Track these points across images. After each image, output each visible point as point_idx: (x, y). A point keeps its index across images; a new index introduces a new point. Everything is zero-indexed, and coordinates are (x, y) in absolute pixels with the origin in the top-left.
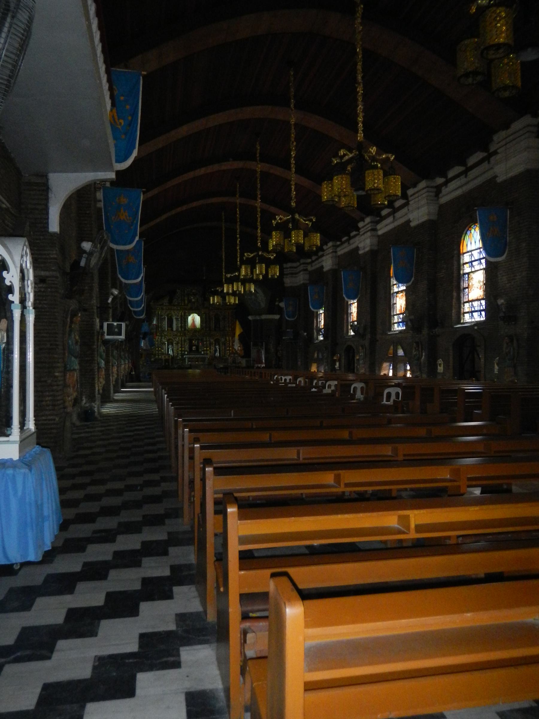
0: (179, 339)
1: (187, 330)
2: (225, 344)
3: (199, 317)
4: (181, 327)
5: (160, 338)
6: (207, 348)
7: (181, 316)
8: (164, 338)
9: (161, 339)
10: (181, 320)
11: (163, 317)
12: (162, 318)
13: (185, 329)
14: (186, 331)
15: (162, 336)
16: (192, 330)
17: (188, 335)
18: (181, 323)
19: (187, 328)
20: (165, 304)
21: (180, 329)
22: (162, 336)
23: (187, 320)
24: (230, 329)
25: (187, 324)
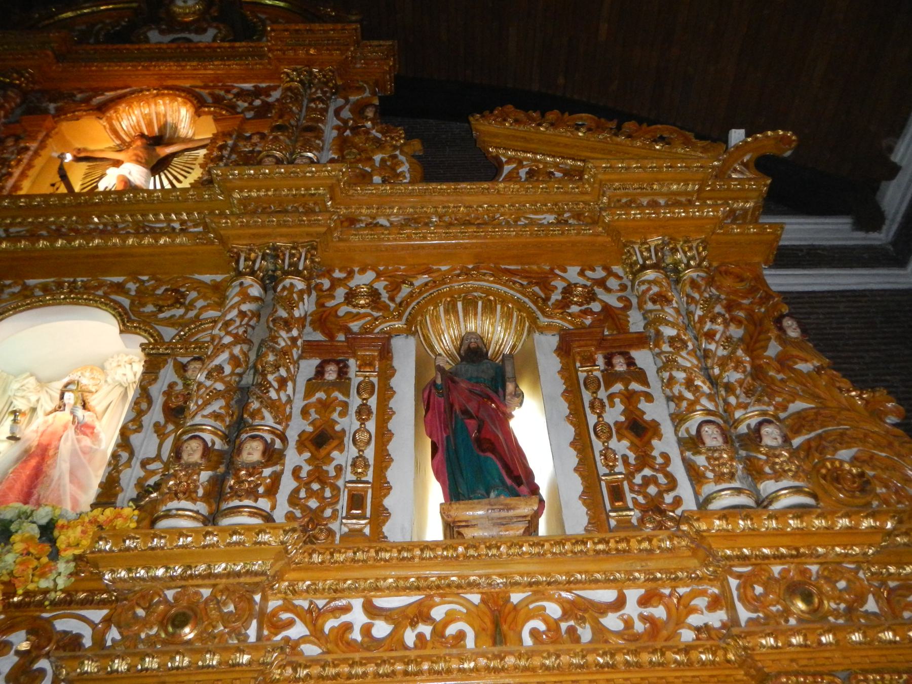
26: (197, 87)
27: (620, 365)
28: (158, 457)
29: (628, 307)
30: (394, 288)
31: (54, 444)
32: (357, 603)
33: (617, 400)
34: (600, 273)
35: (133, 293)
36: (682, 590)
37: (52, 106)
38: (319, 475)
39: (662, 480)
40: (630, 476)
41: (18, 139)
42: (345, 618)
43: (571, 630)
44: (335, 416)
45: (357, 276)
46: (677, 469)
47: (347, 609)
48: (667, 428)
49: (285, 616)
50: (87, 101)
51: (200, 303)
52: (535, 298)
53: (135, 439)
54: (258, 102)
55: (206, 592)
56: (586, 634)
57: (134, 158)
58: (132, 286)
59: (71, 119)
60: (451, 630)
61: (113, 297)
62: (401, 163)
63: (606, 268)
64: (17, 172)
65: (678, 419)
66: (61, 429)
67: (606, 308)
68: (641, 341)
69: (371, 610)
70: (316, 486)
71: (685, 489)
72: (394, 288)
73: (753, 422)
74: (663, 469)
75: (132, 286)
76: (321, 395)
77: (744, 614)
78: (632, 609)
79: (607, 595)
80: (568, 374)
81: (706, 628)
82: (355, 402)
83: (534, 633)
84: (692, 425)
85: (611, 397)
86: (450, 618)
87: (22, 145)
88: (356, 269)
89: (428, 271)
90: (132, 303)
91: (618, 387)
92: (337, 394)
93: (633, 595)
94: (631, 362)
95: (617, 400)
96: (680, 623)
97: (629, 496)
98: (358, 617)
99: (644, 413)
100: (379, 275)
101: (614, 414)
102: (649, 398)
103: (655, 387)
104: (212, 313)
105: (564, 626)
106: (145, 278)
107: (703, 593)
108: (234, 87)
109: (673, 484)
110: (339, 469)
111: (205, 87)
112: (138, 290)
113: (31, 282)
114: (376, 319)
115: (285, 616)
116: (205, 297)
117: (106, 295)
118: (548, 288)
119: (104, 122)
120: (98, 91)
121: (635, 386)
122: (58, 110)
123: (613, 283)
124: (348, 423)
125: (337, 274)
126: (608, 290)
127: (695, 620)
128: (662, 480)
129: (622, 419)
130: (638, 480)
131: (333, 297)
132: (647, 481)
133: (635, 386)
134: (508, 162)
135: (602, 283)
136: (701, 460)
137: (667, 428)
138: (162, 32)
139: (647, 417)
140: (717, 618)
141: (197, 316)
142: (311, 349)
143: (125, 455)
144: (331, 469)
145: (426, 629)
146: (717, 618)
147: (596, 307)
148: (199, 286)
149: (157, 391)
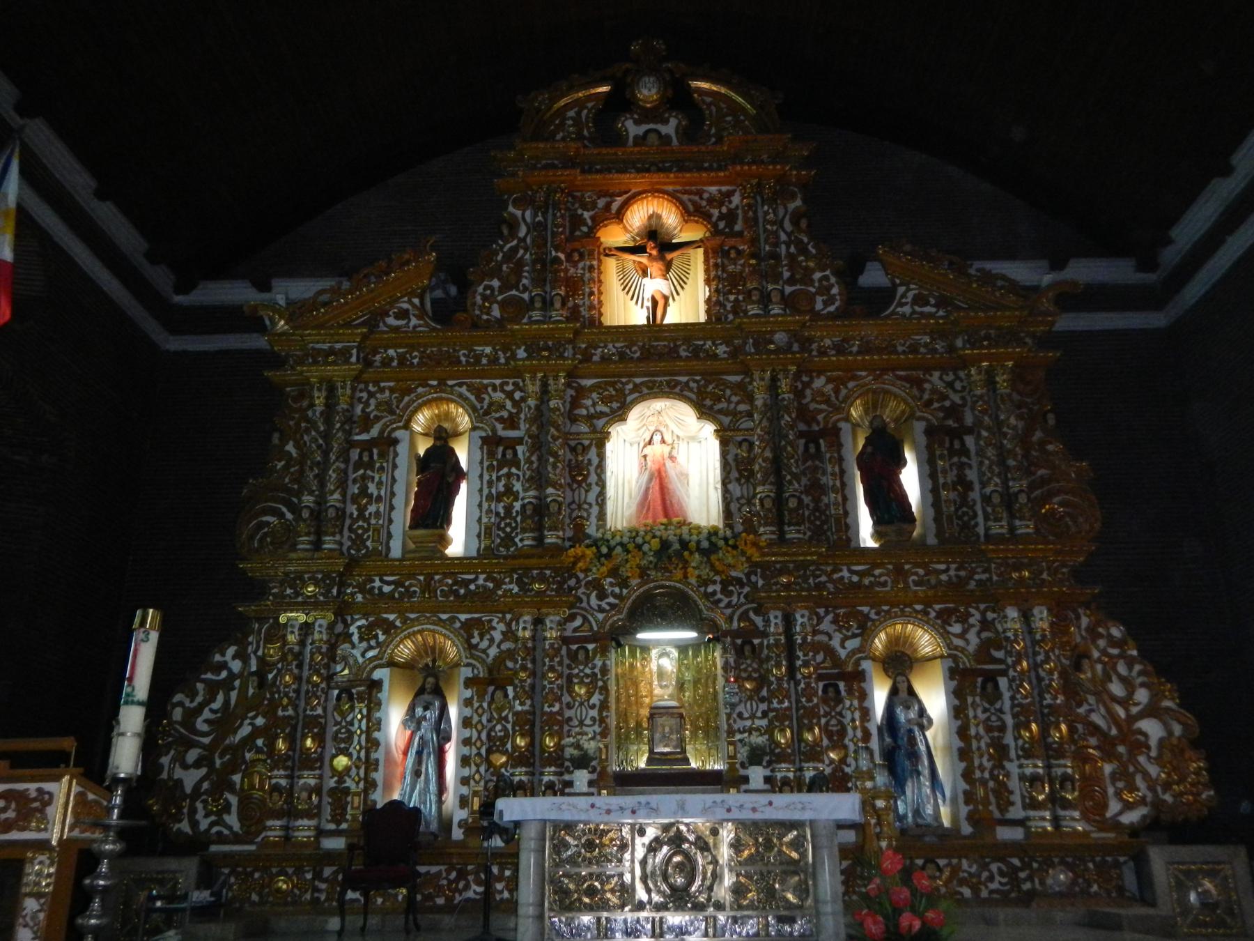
0: (509, 635)
1: (596, 543)
2: (991, 678)
3: (708, 430)
4: (539, 513)
5: (321, 621)
6: (806, 718)
7: (541, 418)
8: (367, 634)
9: (339, 637)
10: (538, 445)
11: (374, 432)
12: (367, 446)
13: (579, 535)
14: (579, 550)
15: (343, 610)
16: (633, 541)
17: (602, 596)
18: (539, 480)
19: (591, 530)
20: (391, 321)
21: (525, 541)
22: (343, 610)
23: (593, 453)
24: (1025, 527)
25: (592, 497)
26: (677, 191)
27: (957, 445)
28: (742, 497)
29: (964, 405)
30: (837, 391)
31: (663, 469)
32: (845, 568)
33: (954, 468)
34: (950, 377)
35: (695, 390)
36: (974, 565)
37: (586, 215)
38: (817, 509)
39: (971, 513)
40: (957, 510)
41: (582, 256)
42: (840, 574)
43: (929, 580)
44: (819, 476)
45: (816, 380)
46: (978, 508)
47: (841, 570)
48: (977, 486)
49: (818, 573)
50: (608, 207)
51: (734, 399)
52: (913, 398)
53: (730, 487)
54: (724, 210)
55: (791, 566)
56: (933, 581)
57: (660, 273)
58: (692, 385)
59: (603, 229)
60: (883, 579)
61: (685, 393)
62: (832, 286)
63: (955, 374)
64: (595, 290)
65: (983, 485)
66: (660, 459)
67: (953, 403)
68: (970, 431)
69: (852, 572)
70: (817, 514)
71: (980, 519)
72: (837, 391)
73: (1016, 489)
74: (972, 507)
75: (692, 385)
76: (809, 463)
77: (995, 578)
78: (952, 573)
79: (943, 567)
80: (929, 447)
81: (981, 580)
82: (829, 469)
83: (913, 581)
84: (988, 490)
85: (951, 465)
86: (881, 575)
87: (588, 263)
88: (814, 374)
89: (854, 378)
90: (698, 397)
91: (955, 459)
92: (817, 463)
93: (953, 566)
94: (963, 443)
95: (954, 468)
96: (971, 578)
97: (955, 521)
98: (845, 573)
99: (966, 476)
100: (829, 381)
101: (952, 476)
102: (970, 467)
103: (974, 463)
104: (742, 407)
105: (926, 578)
106: (698, 378)
107: (980, 567)
108: (705, 191)
109: (975, 515)
110: (828, 506)
111: (686, 192)
112: (698, 388)
113: (638, 380)
114: (831, 412)
115: (818, 573)
116: (736, 395)
117: (682, 390)
118: (922, 391)
119: (621, 226)
120: (613, 195)
121: (964, 459)
122: (593, 218)
123: (958, 385)
124: (826, 480)
125: (805, 379)
126: (955, 391)
127: (977, 577)
128: (971, 513)
129: (955, 479)
130: (960, 513)
131: (805, 397)
132: (965, 514)
133: (964, 459)
134: (901, 285)
135: (950, 385)
136: (989, 509)
137: (977, 486)
138: (637, 123)
139: (968, 479)
140: (984, 576)
141: (735, 408)
142: (801, 435)
143: (728, 495)
144: (822, 505)
145: (872, 579)
146: (984, 576)
147: (947, 404)
148: (727, 385)
149: (730, 458)
